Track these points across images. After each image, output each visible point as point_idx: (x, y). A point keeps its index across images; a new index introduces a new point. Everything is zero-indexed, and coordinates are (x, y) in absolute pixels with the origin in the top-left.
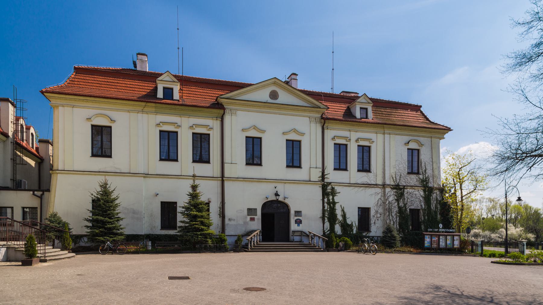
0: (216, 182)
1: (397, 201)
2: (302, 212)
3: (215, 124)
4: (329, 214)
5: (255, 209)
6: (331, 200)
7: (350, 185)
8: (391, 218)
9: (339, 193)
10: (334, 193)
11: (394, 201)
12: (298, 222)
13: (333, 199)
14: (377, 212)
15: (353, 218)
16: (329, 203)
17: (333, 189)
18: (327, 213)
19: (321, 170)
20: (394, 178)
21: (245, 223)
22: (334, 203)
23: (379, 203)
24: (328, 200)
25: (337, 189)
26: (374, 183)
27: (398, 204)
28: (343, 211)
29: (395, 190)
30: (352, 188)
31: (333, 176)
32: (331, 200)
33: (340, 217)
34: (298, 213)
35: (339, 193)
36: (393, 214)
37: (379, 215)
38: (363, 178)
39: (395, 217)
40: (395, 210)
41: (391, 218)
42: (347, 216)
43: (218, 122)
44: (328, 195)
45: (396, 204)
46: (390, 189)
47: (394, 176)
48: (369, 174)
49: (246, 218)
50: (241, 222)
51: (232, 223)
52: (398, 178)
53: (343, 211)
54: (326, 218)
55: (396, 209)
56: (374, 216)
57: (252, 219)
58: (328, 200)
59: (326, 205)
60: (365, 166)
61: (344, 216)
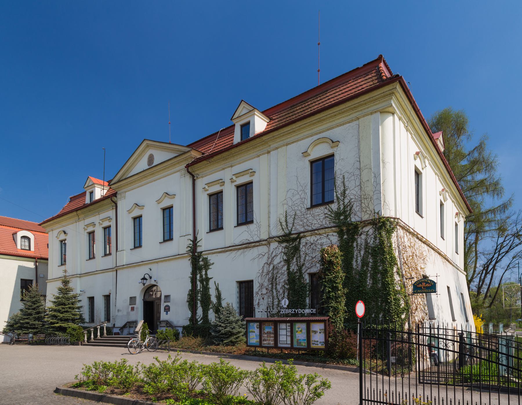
0: (112, 273)
1: (288, 262)
2: (172, 297)
3: (111, 213)
4: (199, 295)
5: (135, 297)
6: (204, 276)
7: (225, 250)
8: (275, 293)
9: (213, 264)
10: (207, 265)
11: (283, 263)
12: (167, 309)
13: (206, 274)
14: (261, 286)
15: (231, 298)
16: (201, 281)
17: (205, 260)
18: (199, 295)
19: (191, 237)
20: (284, 224)
21: (128, 313)
22: (207, 279)
23: (265, 271)
24: (201, 276)
25: (212, 258)
26: (258, 239)
27: (288, 269)
28: (217, 289)
29: (284, 245)
30: (228, 253)
31: (208, 242)
32: (204, 276)
33: (214, 300)
34: (167, 297)
35: (213, 264)
36: (279, 287)
37: (264, 291)
38: (245, 234)
39: (281, 291)
40: (283, 278)
41: (275, 293)
42: (223, 296)
43: (114, 210)
44: (200, 269)
45: (285, 268)
46: (276, 244)
47: (283, 220)
48: (251, 226)
49: (129, 307)
50: (125, 313)
51: (120, 314)
52: (290, 220)
53: (217, 289)
54: (199, 302)
55: (285, 277)
56: (257, 293)
57: (133, 309)
58: (201, 276)
59: (198, 283)
60: (245, 218)
61: (219, 297)
